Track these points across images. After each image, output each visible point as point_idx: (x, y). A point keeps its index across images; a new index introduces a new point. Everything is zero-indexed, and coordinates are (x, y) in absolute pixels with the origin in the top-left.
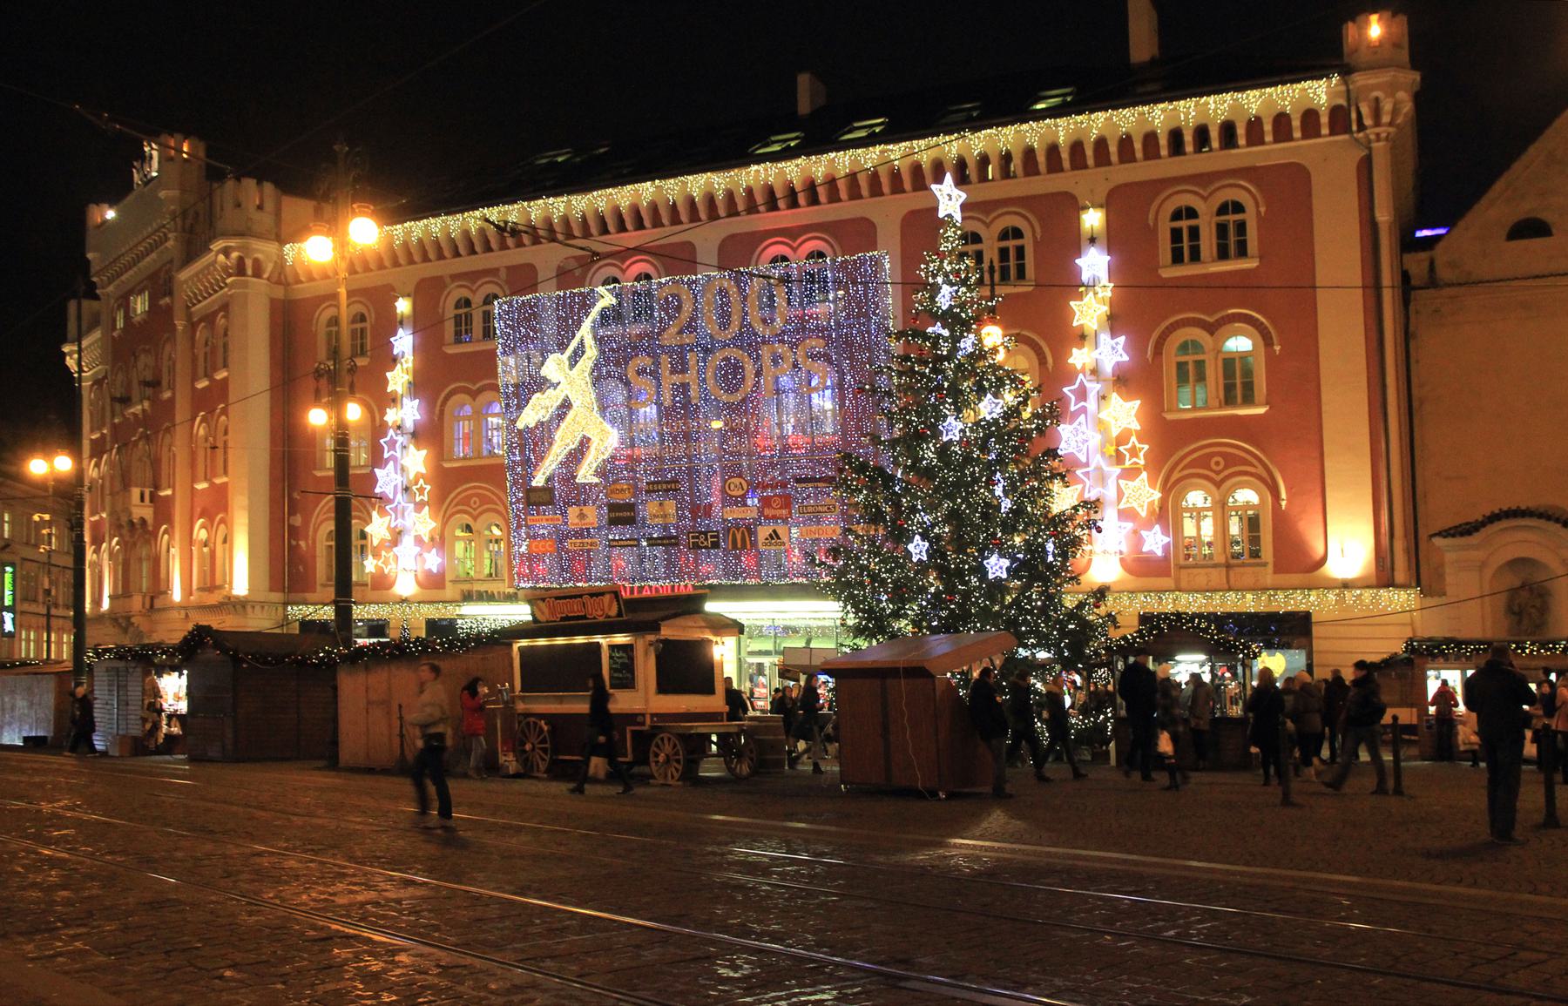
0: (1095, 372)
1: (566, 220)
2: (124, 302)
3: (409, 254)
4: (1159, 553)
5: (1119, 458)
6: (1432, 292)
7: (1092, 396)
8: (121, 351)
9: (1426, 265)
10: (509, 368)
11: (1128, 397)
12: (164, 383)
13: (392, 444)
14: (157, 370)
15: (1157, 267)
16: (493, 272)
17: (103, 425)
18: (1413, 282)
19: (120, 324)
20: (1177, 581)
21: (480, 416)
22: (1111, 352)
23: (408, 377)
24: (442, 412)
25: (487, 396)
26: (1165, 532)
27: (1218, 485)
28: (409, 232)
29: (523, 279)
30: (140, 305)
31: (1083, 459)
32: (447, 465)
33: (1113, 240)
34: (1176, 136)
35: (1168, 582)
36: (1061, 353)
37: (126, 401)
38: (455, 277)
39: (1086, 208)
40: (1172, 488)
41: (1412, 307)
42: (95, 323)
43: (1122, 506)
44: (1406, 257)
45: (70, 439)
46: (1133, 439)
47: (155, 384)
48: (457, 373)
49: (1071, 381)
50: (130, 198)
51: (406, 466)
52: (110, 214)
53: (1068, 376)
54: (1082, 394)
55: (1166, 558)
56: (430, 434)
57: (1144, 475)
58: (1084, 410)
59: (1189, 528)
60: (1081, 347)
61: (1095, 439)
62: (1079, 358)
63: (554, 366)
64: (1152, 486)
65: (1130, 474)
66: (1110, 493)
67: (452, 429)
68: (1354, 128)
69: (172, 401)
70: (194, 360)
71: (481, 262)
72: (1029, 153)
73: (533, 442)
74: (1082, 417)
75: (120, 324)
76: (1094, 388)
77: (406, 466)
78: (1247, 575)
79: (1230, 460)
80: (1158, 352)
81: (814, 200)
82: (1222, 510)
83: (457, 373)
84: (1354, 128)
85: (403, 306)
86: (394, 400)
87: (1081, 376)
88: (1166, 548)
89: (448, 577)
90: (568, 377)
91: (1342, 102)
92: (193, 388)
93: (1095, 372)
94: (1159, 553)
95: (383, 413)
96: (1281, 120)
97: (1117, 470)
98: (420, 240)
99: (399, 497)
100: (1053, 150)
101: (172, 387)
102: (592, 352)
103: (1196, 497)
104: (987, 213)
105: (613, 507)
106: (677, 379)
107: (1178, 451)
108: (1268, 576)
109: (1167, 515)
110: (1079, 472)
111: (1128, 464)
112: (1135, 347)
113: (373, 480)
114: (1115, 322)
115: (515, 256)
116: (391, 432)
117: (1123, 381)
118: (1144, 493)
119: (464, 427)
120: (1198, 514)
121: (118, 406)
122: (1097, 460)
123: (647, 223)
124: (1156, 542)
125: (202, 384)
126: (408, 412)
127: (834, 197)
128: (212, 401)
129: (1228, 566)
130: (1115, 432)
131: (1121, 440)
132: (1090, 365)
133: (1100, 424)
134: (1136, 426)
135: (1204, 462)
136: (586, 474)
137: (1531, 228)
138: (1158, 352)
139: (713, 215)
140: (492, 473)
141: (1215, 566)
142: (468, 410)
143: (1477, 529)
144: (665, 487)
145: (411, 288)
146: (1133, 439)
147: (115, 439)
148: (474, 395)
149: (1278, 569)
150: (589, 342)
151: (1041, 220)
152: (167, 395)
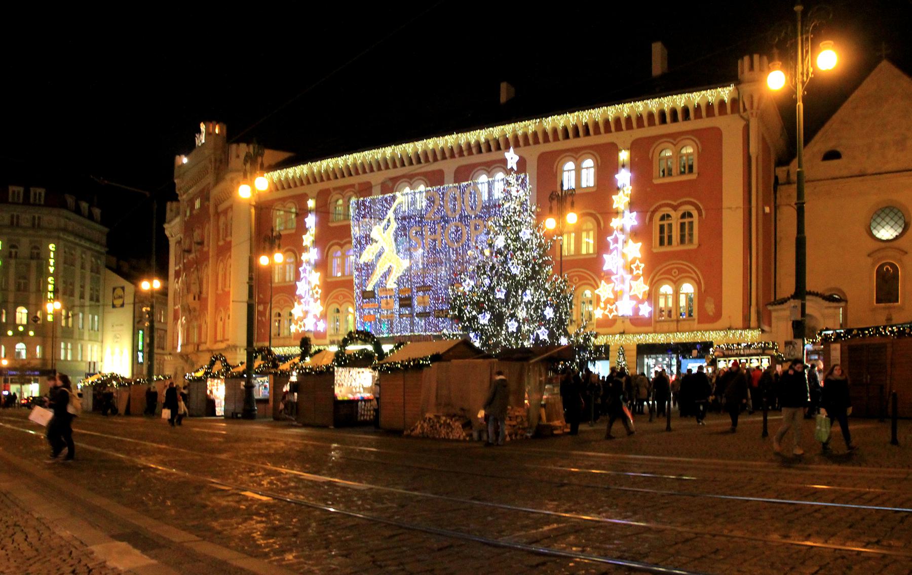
0: (622, 230)
1: (355, 165)
2: (191, 203)
3: (321, 177)
4: (647, 315)
5: (631, 271)
6: (786, 186)
7: (620, 241)
8: (188, 228)
9: (785, 173)
10: (356, 231)
11: (636, 241)
12: (206, 243)
13: (305, 270)
14: (203, 236)
15: (652, 178)
16: (352, 186)
17: (180, 263)
18: (780, 182)
19: (188, 214)
20: (655, 327)
21: (344, 257)
22: (630, 220)
23: (312, 238)
24: (327, 256)
25: (347, 246)
26: (650, 305)
27: (675, 282)
28: (311, 168)
29: (365, 190)
30: (197, 204)
31: (615, 272)
32: (329, 280)
33: (633, 165)
34: (662, 114)
35: (651, 329)
36: (607, 221)
37: (189, 251)
38: (335, 189)
39: (621, 150)
40: (654, 284)
41: (778, 195)
42: (178, 214)
43: (632, 293)
44: (777, 169)
45: (162, 272)
46: (638, 262)
47: (201, 243)
48: (334, 236)
49: (611, 234)
50: (194, 152)
51: (310, 282)
52: (185, 160)
53: (609, 231)
54: (616, 240)
55: (650, 318)
56: (322, 265)
57: (642, 278)
58: (616, 248)
59: (662, 304)
60: (616, 217)
61: (621, 262)
62: (615, 223)
63: (377, 232)
64: (645, 283)
65: (636, 278)
66: (627, 288)
67: (332, 262)
68: (741, 110)
69: (208, 252)
70: (218, 230)
71: (348, 181)
72: (596, 124)
73: (368, 269)
74: (615, 252)
75: (188, 214)
76: (621, 237)
77: (310, 282)
78: (686, 325)
79: (681, 271)
80: (651, 219)
81: (470, 153)
82: (677, 294)
83: (334, 236)
84: (741, 110)
85: (311, 203)
86: (306, 249)
87: (615, 232)
88: (650, 313)
89: (328, 334)
90: (383, 235)
91: (736, 96)
92: (218, 246)
93: (622, 230)
94: (647, 315)
95: (301, 255)
96: (709, 106)
97: (630, 276)
98: (333, 169)
99: (307, 296)
100: (607, 122)
101: (208, 246)
102: (394, 225)
103: (666, 288)
104: (577, 153)
105: (401, 299)
106: (433, 237)
107: (659, 268)
108: (695, 325)
109: (652, 296)
110: (613, 278)
111: (635, 273)
112: (641, 217)
113: (294, 288)
114: (632, 206)
115: (363, 178)
116: (304, 265)
117: (635, 234)
118: (641, 287)
119: (337, 261)
120: (666, 296)
121: (186, 254)
122: (622, 272)
123: (422, 161)
124: (645, 310)
125: (221, 243)
126: (312, 255)
127: (556, 138)
128: (224, 250)
129: (678, 321)
130: (630, 259)
131: (633, 262)
132: (620, 226)
133: (623, 255)
134: (639, 255)
135: (669, 272)
136: (391, 284)
137: (833, 155)
138: (651, 219)
139: (536, 142)
140: (347, 284)
141: (672, 321)
142: (339, 254)
143: (786, 301)
144: (425, 288)
145: (315, 194)
146: (638, 262)
147: (185, 270)
148: (342, 246)
149: (699, 322)
150: (392, 220)
151: (702, 143)
152: (205, 249)
